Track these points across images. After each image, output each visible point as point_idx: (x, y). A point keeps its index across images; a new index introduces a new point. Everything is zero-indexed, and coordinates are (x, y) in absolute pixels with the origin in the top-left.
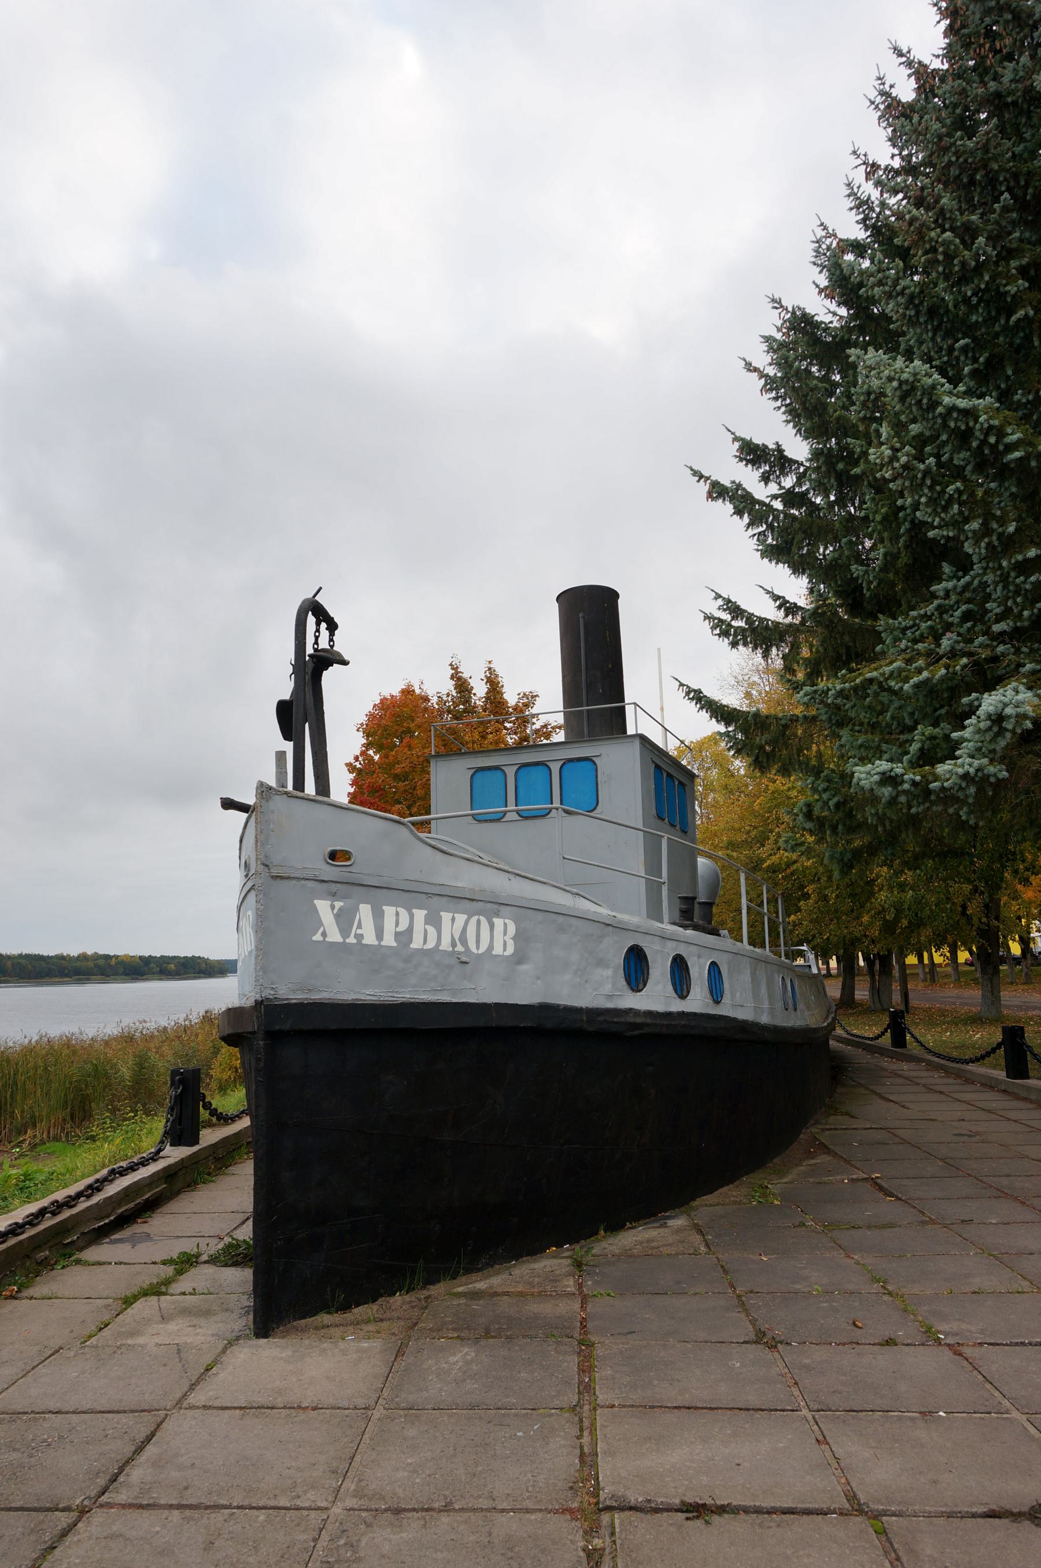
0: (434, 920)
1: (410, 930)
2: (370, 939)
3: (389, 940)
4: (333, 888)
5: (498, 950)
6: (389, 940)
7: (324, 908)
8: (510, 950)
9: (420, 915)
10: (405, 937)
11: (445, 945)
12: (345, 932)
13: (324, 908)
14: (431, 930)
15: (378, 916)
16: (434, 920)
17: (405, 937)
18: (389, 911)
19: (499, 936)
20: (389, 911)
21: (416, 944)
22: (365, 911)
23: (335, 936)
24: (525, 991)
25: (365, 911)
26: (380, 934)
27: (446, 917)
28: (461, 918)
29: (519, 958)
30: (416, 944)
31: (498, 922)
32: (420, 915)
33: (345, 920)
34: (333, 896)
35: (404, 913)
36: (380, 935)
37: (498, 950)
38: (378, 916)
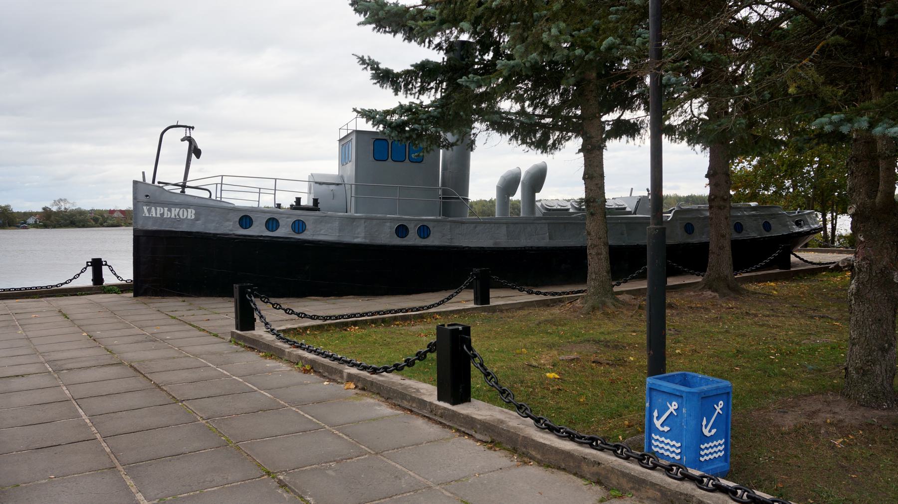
0: (170, 210)
3: (158, 215)
4: (148, 204)
5: (189, 217)
6: (158, 215)
7: (145, 208)
8: (193, 217)
9: (166, 209)
10: (162, 215)
11: (173, 216)
13: (145, 208)
15: (156, 210)
16: (170, 210)
17: (162, 215)
18: (158, 209)
19: (190, 214)
20: (158, 209)
21: (165, 216)
24: (199, 227)
27: (173, 209)
28: (178, 210)
29: (197, 219)
30: (165, 216)
31: (189, 210)
32: (166, 209)
33: (149, 211)
38: (156, 210)
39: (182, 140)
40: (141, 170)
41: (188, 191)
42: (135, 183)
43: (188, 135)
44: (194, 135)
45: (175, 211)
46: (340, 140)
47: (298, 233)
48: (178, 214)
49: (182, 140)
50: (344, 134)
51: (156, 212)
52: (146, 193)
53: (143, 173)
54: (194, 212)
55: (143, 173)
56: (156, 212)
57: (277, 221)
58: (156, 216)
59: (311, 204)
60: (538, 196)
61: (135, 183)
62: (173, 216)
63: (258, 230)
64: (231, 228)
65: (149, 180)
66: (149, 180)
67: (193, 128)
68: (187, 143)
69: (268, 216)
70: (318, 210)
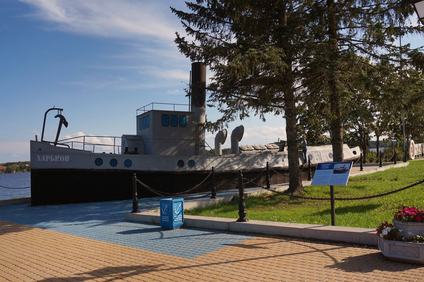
0: (54, 157)
1: (50, 158)
2: (44, 160)
3: (47, 160)
5: (66, 161)
6: (47, 160)
7: (38, 156)
8: (68, 160)
9: (52, 156)
11: (56, 160)
12: (41, 159)
14: (54, 159)
16: (54, 157)
18: (47, 156)
19: (67, 159)
20: (47, 156)
21: (51, 160)
22: (44, 156)
23: (40, 160)
25: (44, 156)
26: (46, 159)
27: (56, 156)
28: (59, 156)
30: (51, 160)
31: (66, 157)
32: (52, 156)
33: (41, 158)
34: (39, 155)
35: (49, 157)
36: (46, 159)
37: (66, 161)
39: (56, 117)
40: (35, 133)
41: (57, 146)
42: (31, 142)
43: (60, 114)
44: (63, 114)
45: (57, 158)
46: (137, 116)
47: (128, 167)
48: (59, 159)
49: (56, 117)
50: (140, 113)
51: (46, 158)
52: (38, 147)
53: (36, 136)
54: (68, 157)
55: (36, 136)
56: (46, 158)
57: (116, 161)
58: (49, 161)
59: (134, 151)
60: (241, 144)
61: (31, 142)
62: (56, 160)
63: (106, 166)
64: (91, 165)
65: (39, 140)
66: (39, 140)
67: (62, 110)
68: (59, 119)
69: (113, 158)
70: (137, 154)
